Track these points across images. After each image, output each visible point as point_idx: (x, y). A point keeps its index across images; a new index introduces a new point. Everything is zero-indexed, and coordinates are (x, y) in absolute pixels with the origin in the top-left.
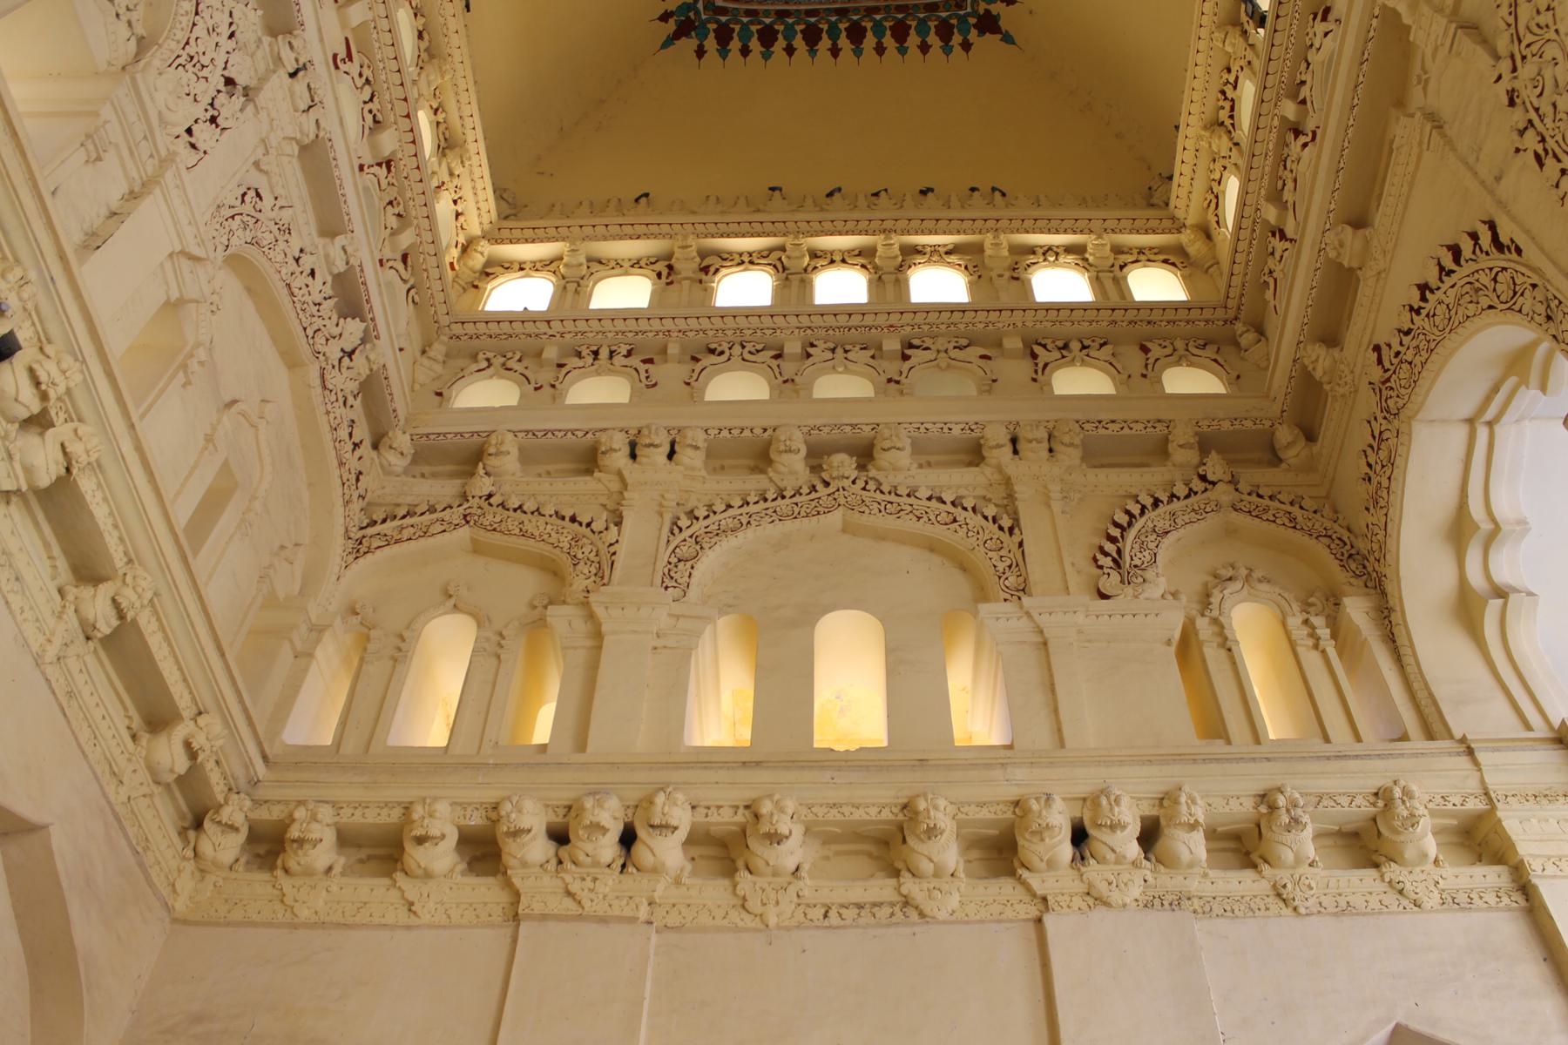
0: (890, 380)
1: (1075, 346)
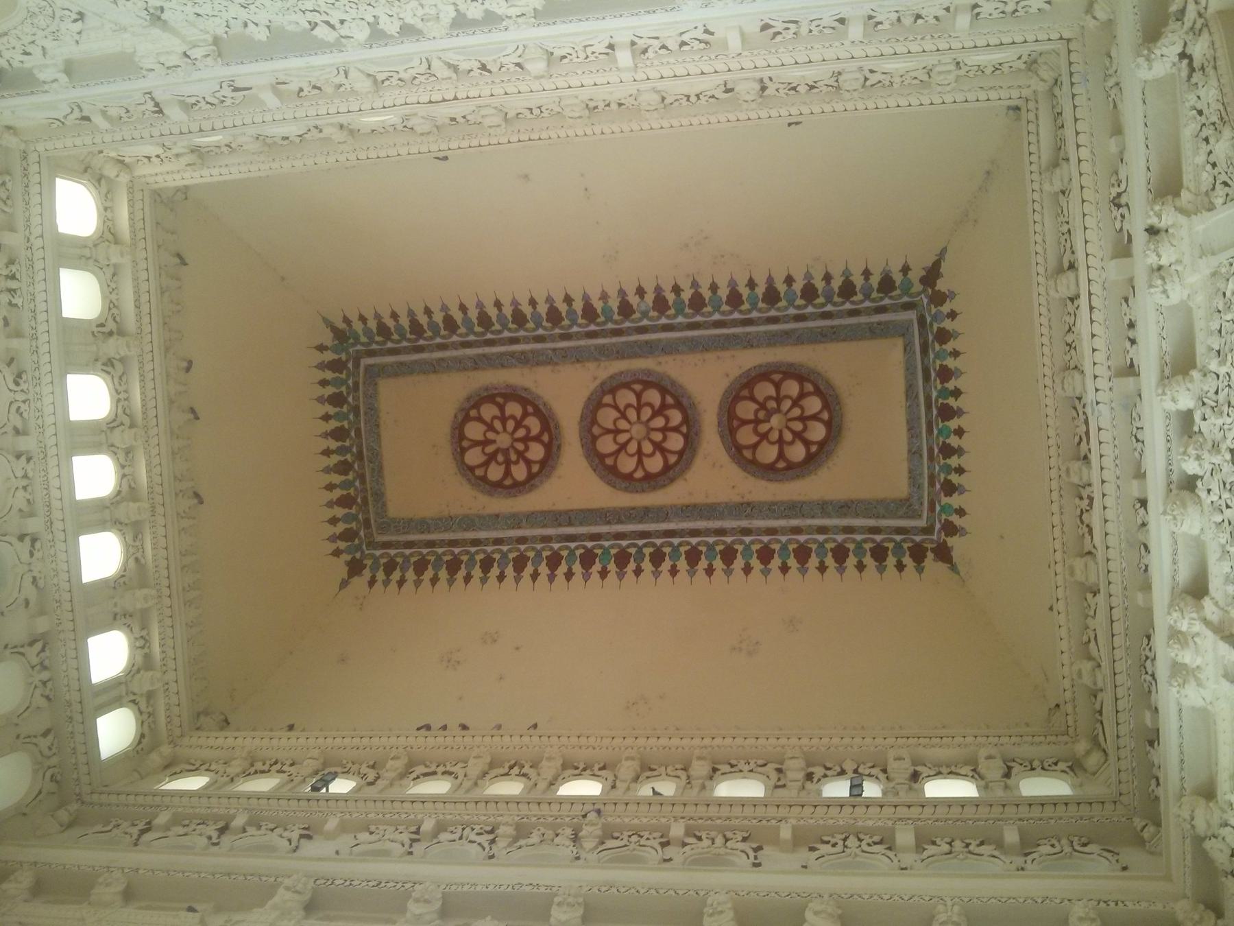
1: (45, 675)
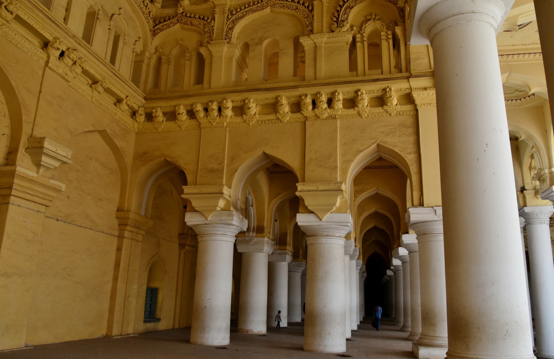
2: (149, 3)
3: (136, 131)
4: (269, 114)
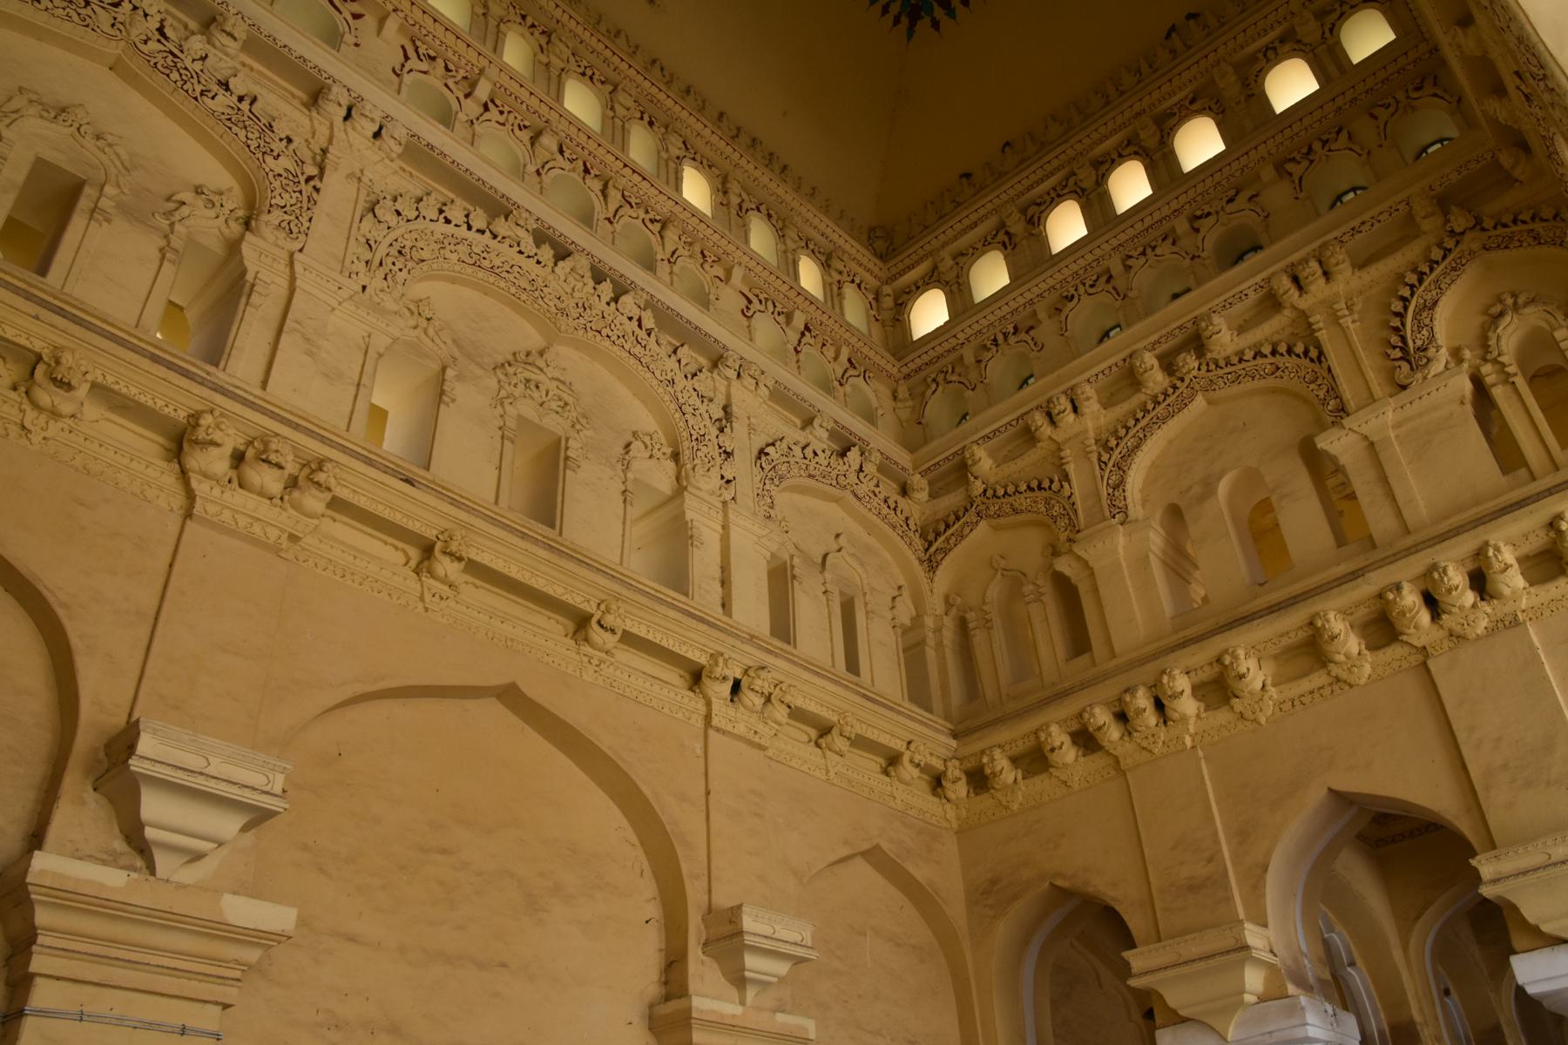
0: (1193, 258)
1: (1317, 146)
2: (899, 499)
3: (955, 826)
4: (1306, 674)
